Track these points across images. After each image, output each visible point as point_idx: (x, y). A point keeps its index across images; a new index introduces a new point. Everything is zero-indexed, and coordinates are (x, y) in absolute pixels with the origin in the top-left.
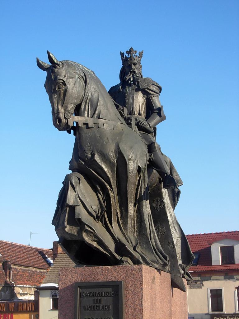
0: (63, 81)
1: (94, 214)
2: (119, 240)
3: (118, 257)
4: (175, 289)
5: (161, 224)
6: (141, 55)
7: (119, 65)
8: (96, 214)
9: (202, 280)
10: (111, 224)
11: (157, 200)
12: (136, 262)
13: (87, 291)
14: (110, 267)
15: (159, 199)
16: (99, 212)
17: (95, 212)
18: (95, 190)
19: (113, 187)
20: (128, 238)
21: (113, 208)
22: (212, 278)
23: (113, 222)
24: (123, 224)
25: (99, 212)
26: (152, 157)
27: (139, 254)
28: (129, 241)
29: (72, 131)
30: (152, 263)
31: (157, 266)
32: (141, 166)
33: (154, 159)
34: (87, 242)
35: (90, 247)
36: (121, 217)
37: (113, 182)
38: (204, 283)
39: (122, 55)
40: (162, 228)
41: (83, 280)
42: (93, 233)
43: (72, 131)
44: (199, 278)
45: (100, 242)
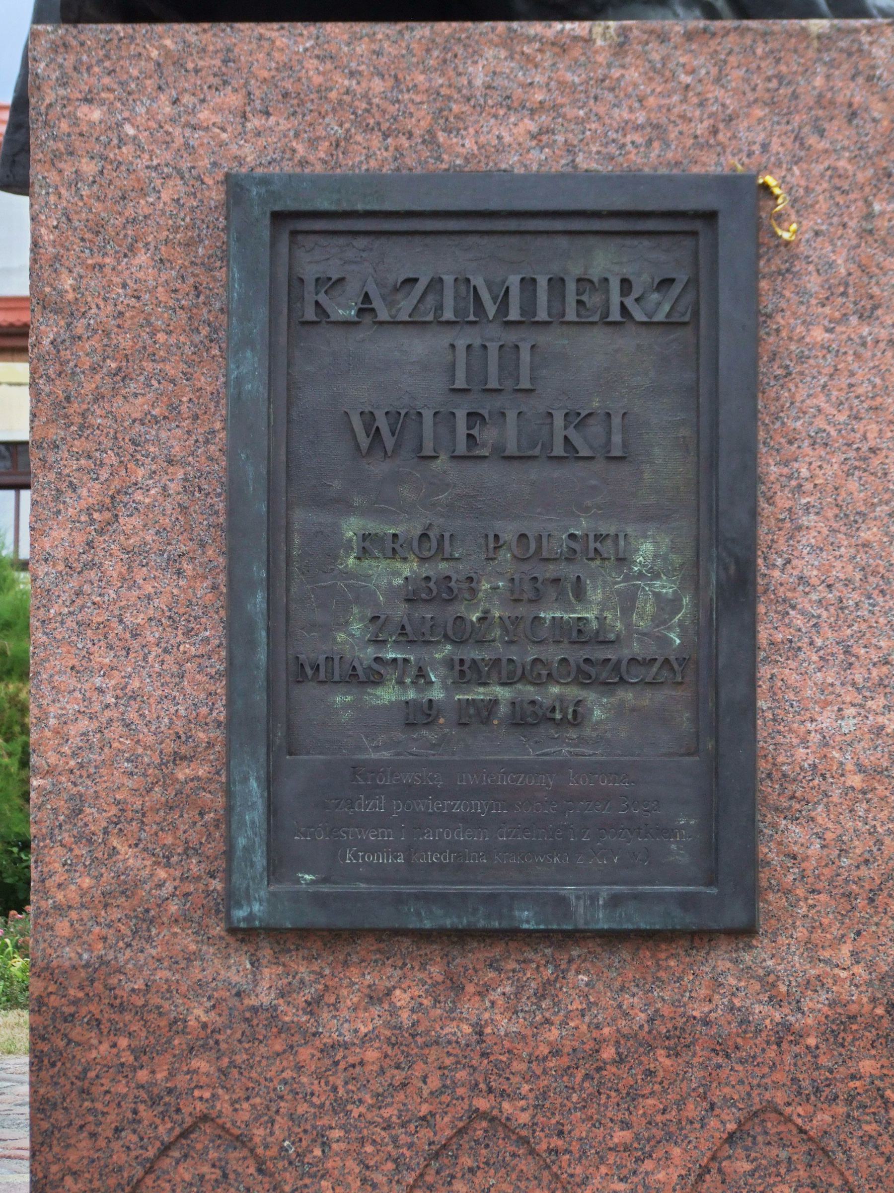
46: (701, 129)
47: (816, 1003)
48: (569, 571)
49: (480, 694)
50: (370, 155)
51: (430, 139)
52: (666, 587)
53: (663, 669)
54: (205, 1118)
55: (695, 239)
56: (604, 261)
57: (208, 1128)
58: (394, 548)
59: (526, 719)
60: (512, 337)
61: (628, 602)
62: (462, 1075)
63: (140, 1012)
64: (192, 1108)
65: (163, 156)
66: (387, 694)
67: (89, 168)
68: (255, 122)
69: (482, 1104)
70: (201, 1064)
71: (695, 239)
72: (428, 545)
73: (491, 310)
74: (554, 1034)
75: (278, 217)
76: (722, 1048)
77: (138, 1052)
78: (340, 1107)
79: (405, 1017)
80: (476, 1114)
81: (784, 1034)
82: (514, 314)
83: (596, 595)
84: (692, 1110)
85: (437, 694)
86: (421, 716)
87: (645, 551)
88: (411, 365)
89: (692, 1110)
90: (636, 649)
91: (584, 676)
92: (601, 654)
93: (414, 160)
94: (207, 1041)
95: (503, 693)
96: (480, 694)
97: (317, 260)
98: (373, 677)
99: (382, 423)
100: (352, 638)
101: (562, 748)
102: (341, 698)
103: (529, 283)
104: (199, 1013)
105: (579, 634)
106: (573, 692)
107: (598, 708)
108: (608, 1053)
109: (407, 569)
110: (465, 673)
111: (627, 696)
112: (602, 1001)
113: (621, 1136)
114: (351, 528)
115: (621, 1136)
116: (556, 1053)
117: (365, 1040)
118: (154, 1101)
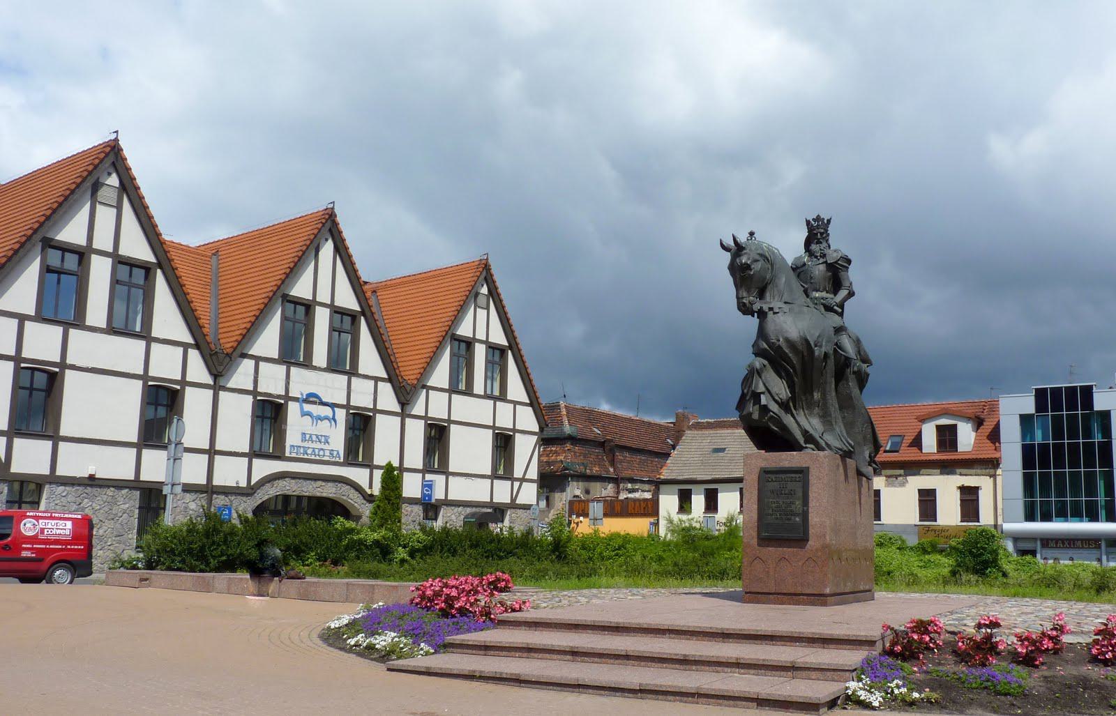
3: (804, 446)
6: (829, 221)
7: (805, 234)
9: (906, 475)
12: (820, 448)
13: (773, 477)
14: (795, 453)
17: (781, 400)
18: (781, 377)
22: (921, 473)
29: (756, 314)
31: (841, 453)
37: (798, 367)
38: (909, 478)
39: (808, 223)
41: (768, 466)
43: (756, 314)
44: (902, 472)
45: (784, 428)
52: (799, 506)
55: (803, 472)
61: (796, 508)
71: (803, 472)
87: (797, 503)
88: (774, 486)
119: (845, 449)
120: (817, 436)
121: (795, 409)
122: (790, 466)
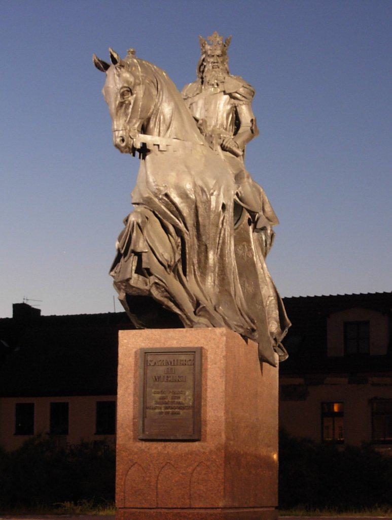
0: (129, 89)
1: (166, 264)
2: (196, 297)
3: (195, 319)
4: (265, 364)
5: (247, 278)
8: (168, 264)
10: (185, 275)
11: (244, 246)
15: (245, 243)
16: (171, 261)
19: (189, 228)
20: (207, 296)
21: (189, 256)
23: (187, 273)
24: (201, 276)
25: (171, 261)
26: (241, 190)
27: (221, 315)
28: (208, 299)
30: (236, 327)
31: (241, 330)
32: (225, 203)
33: (242, 192)
34: (155, 298)
35: (159, 304)
36: (199, 267)
40: (249, 284)
42: (164, 287)
43: (137, 154)
45: (172, 298)
46: (196, 341)
47: (208, 449)
48: (178, 395)
49: (168, 410)
50: (157, 345)
51: (164, 344)
53: (189, 408)
54: (136, 463)
56: (183, 357)
57: (136, 464)
58: (158, 393)
59: (173, 413)
60: (172, 367)
61: (185, 399)
62: (166, 458)
63: (129, 450)
64: (135, 461)
65: (134, 346)
66: (157, 411)
67: (125, 347)
68: (144, 341)
69: (169, 461)
70: (136, 456)
71: (196, 356)
72: (162, 392)
73: (169, 363)
74: (177, 453)
75: (145, 353)
76: (197, 454)
77: (129, 454)
78: (151, 461)
79: (160, 450)
80: (167, 463)
81: (204, 453)
82: (172, 364)
83: (181, 398)
84: (193, 462)
85: (163, 411)
86: (161, 413)
87: (187, 393)
89: (193, 462)
90: (186, 405)
91: (179, 408)
92: (182, 405)
93: (162, 346)
94: (136, 453)
95: (170, 410)
96: (168, 410)
97: (149, 358)
98: (155, 409)
99: (157, 378)
100: (153, 404)
101: (177, 417)
102: (152, 411)
103: (174, 360)
104: (136, 450)
105: (179, 403)
106: (179, 410)
107: (181, 412)
108: (183, 455)
109: (160, 395)
110: (166, 408)
111: (185, 411)
112: (183, 447)
113: (185, 465)
114: (153, 391)
115: (185, 465)
116: (177, 455)
117: (155, 453)
118: (130, 461)
119: (246, 326)
120: (210, 309)
121: (185, 275)
122: (179, 346)
